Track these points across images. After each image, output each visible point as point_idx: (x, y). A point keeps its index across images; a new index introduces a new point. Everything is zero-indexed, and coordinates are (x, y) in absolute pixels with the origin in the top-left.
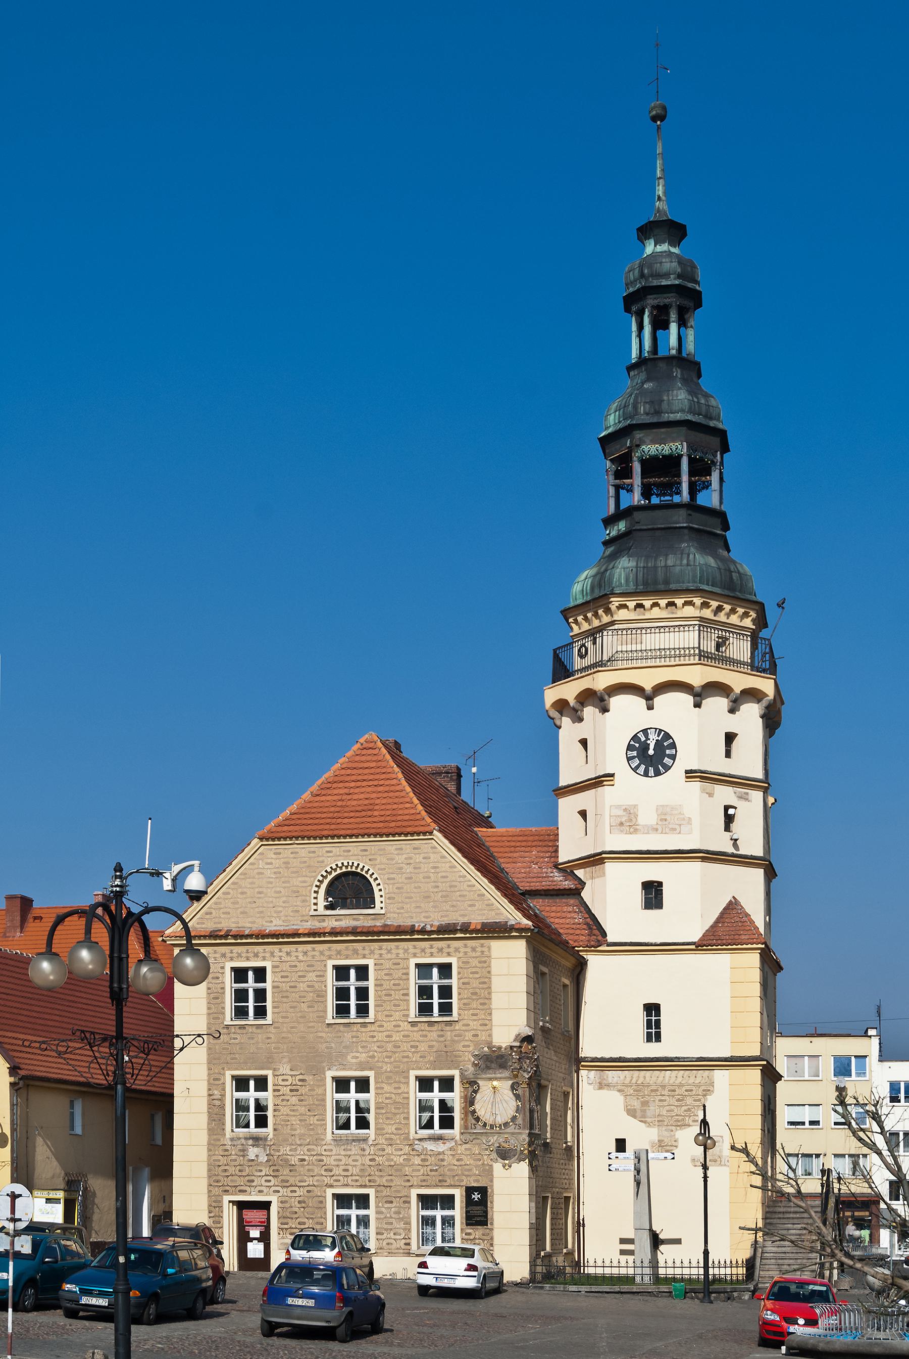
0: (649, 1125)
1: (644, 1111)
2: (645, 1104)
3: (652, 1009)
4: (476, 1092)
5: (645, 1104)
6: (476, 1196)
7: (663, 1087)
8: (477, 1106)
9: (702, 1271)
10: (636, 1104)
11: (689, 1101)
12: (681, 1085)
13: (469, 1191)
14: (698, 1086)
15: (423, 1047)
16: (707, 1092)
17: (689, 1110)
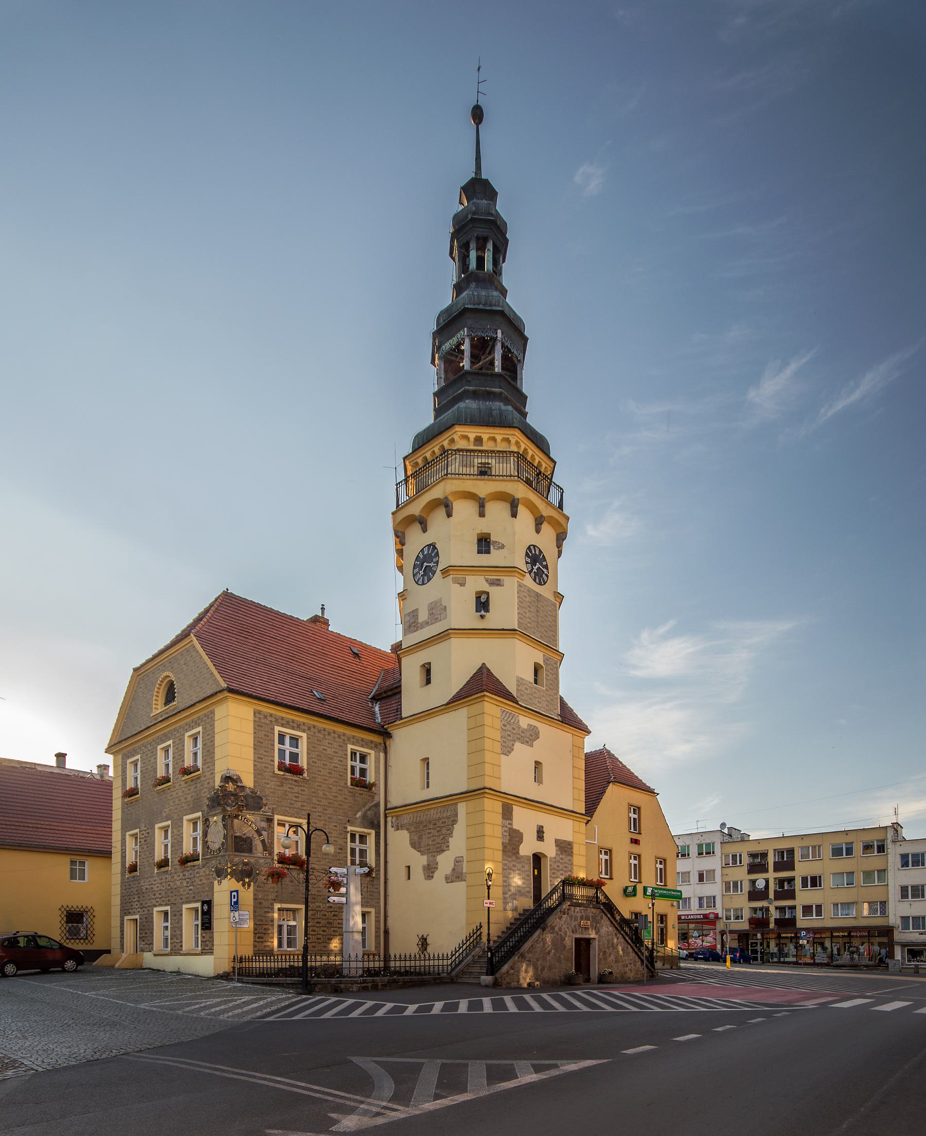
0: (422, 853)
1: (419, 843)
2: (420, 837)
3: (426, 761)
4: (208, 827)
5: (420, 837)
6: (206, 907)
7: (430, 822)
8: (208, 838)
9: (301, 964)
10: (416, 838)
11: (444, 831)
12: (440, 819)
13: (203, 903)
14: (448, 818)
15: (189, 799)
16: (455, 822)
17: (444, 838)
